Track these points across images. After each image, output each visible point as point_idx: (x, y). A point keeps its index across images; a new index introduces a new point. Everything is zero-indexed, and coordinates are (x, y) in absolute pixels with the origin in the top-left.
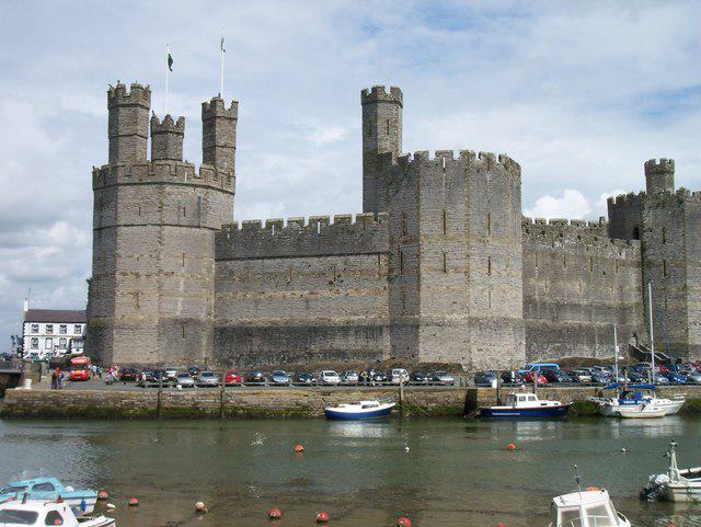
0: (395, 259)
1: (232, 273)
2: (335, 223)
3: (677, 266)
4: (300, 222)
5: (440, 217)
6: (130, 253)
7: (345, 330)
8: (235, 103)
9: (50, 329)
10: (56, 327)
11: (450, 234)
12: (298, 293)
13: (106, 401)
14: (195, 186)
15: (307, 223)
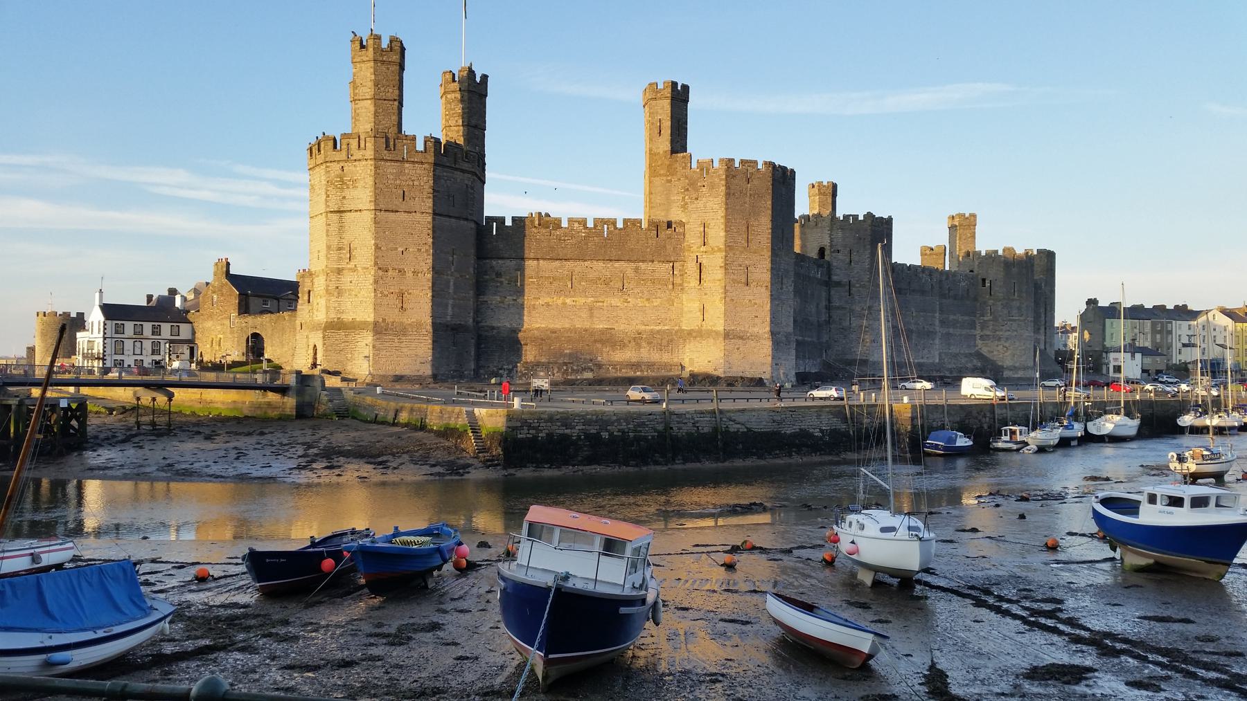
0: (691, 267)
1: (499, 275)
2: (595, 226)
3: (863, 286)
4: (583, 222)
5: (744, 228)
6: (391, 245)
7: (637, 339)
8: (485, 78)
9: (139, 332)
10: (148, 327)
11: (753, 246)
12: (581, 300)
13: (618, 420)
14: (463, 171)
15: (590, 224)
